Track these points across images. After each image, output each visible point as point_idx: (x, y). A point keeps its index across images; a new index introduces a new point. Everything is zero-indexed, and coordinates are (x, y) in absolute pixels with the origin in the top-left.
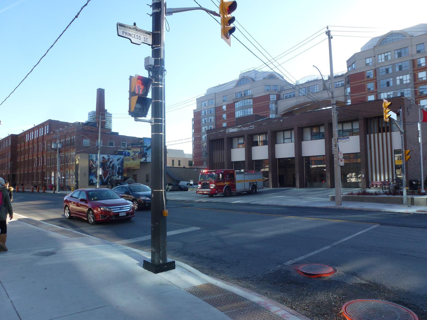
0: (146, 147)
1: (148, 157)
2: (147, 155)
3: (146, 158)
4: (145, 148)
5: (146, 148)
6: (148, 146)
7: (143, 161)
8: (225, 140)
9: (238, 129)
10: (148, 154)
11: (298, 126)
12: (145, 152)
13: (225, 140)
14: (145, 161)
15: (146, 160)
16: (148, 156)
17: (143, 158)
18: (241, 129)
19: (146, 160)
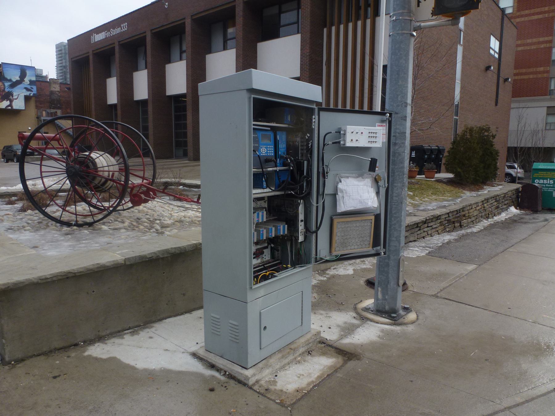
0: (10, 80)
1: (15, 99)
2: (13, 97)
3: (11, 101)
4: (7, 82)
5: (9, 83)
6: (14, 80)
7: (4, 108)
8: (91, 58)
9: (106, 32)
10: (14, 94)
11: (192, 16)
12: (7, 90)
13: (91, 58)
14: (10, 108)
15: (10, 105)
16: (14, 97)
17: (5, 101)
18: (111, 33)
19: (10, 105)
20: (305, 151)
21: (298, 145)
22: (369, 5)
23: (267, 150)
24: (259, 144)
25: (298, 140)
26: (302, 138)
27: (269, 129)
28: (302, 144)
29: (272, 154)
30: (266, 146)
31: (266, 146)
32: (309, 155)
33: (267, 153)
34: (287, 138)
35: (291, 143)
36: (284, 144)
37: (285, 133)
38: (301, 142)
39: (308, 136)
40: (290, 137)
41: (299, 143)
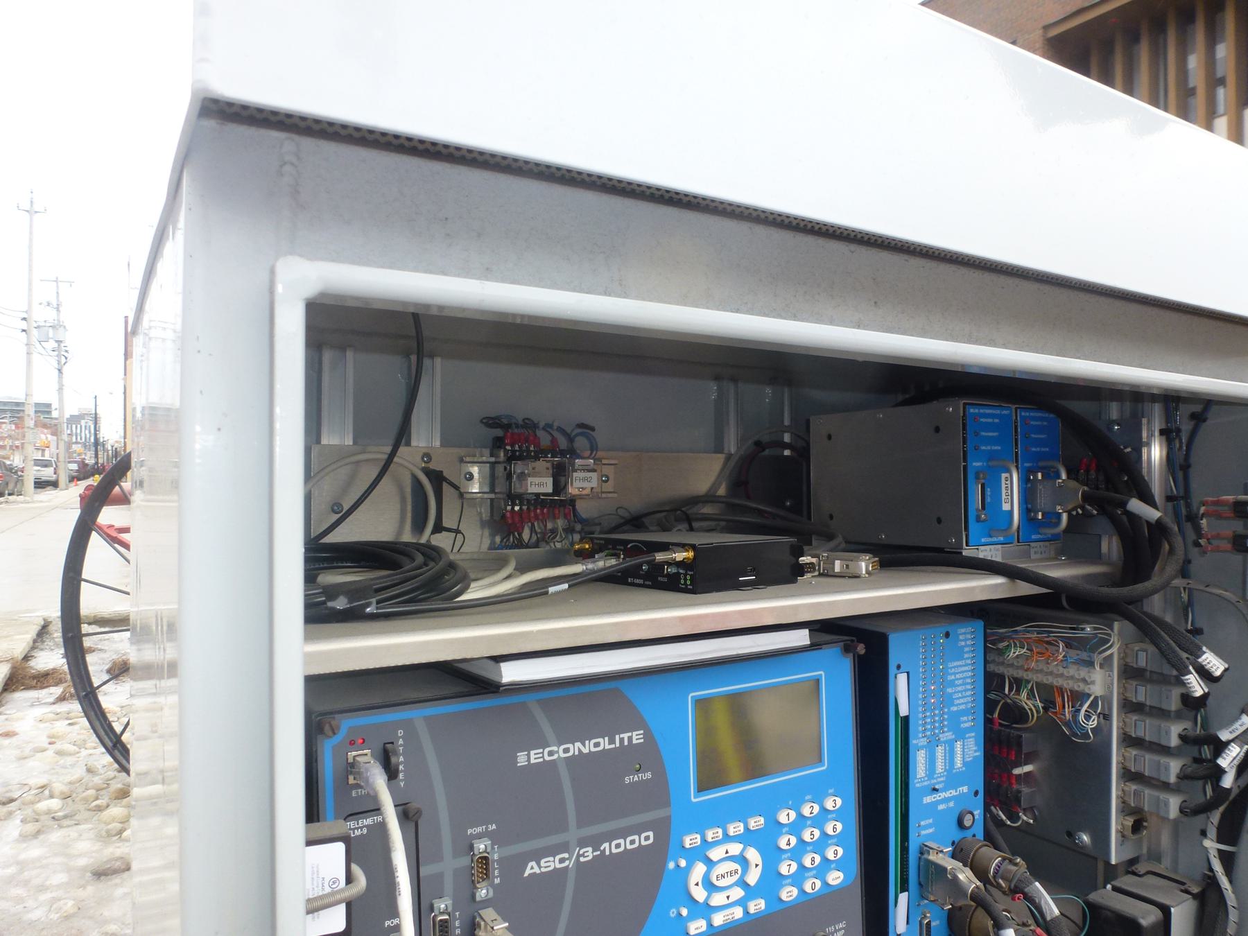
20: (1173, 804)
21: (1102, 732)
22: (1222, 82)
23: (772, 855)
24: (663, 829)
25: (1097, 690)
26: (1130, 673)
27: (801, 638)
28: (1144, 728)
29: (835, 878)
30: (756, 822)
31: (756, 822)
32: (1211, 845)
33: (772, 878)
34: (992, 682)
35: (1030, 703)
36: (960, 735)
37: (968, 635)
38: (1130, 707)
39: (1204, 674)
40: (1013, 653)
41: (1106, 717)
